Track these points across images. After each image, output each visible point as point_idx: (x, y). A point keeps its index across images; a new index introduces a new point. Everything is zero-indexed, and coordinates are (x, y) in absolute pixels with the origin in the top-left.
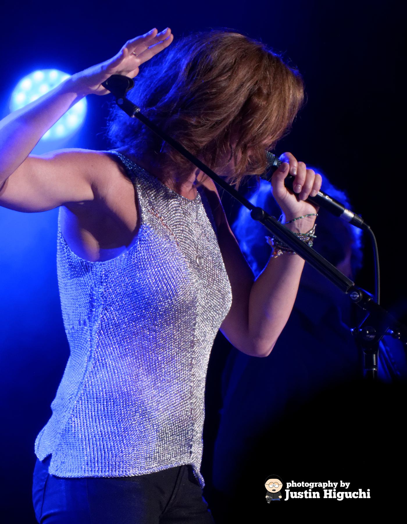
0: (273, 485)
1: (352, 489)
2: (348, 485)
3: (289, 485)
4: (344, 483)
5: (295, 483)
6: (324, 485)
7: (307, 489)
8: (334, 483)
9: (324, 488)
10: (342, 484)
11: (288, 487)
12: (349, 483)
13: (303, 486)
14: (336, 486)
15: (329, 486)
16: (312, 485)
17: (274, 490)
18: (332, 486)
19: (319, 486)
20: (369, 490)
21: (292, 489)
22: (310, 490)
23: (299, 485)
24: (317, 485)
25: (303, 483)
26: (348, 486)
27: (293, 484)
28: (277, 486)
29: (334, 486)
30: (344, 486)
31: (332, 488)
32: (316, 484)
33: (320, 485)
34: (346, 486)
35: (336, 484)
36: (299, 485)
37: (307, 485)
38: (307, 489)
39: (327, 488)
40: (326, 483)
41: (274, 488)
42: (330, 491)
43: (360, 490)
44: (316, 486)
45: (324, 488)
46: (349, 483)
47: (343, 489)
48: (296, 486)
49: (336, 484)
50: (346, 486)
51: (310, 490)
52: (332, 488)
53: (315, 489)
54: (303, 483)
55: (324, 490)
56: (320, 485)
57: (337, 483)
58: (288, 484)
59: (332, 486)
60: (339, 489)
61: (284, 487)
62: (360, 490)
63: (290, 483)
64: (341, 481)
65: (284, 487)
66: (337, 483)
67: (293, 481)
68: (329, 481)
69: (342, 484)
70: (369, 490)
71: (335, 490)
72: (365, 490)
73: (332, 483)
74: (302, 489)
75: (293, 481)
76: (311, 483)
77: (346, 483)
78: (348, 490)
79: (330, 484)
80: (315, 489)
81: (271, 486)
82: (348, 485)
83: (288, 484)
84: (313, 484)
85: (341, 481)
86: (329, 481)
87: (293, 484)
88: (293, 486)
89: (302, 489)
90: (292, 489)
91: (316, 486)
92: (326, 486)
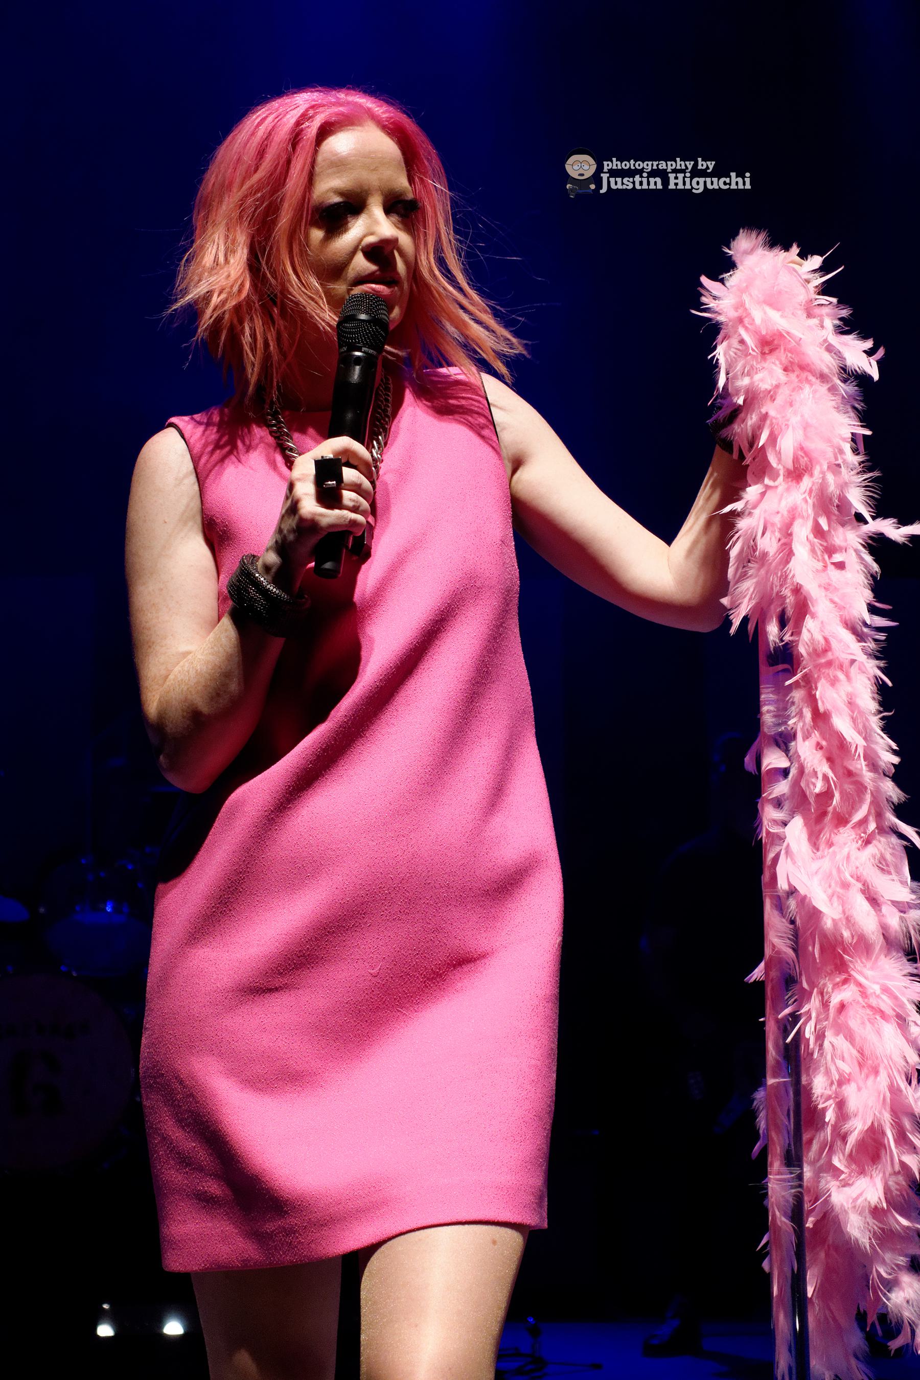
0: (580, 166)
1: (718, 173)
2: (711, 165)
4: (704, 163)
5: (619, 163)
6: (670, 166)
7: (640, 172)
8: (687, 163)
9: (669, 170)
10: (702, 164)
11: (606, 169)
12: (713, 163)
13: (633, 168)
14: (690, 167)
15: (678, 167)
16: (648, 166)
17: (582, 175)
18: (683, 167)
19: (660, 167)
20: (748, 174)
21: (613, 173)
22: (645, 175)
24: (657, 165)
25: (632, 162)
26: (711, 167)
27: (615, 164)
28: (586, 167)
29: (687, 168)
30: (704, 167)
31: (683, 171)
32: (655, 163)
33: (663, 165)
34: (708, 168)
35: (690, 165)
37: (640, 165)
38: (640, 172)
39: (675, 171)
40: (673, 163)
41: (581, 172)
42: (681, 176)
43: (733, 175)
44: (655, 167)
45: (669, 170)
46: (713, 163)
47: (703, 173)
48: (619, 167)
49: (690, 165)
50: (708, 168)
51: (645, 175)
52: (683, 171)
53: (653, 173)
54: (632, 162)
55: (670, 175)
56: (663, 165)
57: (692, 163)
58: (605, 163)
59: (683, 167)
61: (600, 169)
62: (733, 175)
63: (610, 163)
64: (700, 159)
65: (600, 169)
66: (692, 163)
67: (614, 159)
68: (678, 159)
69: (702, 164)
70: (748, 174)
71: (688, 175)
72: (741, 175)
73: (683, 163)
74: (631, 173)
75: (614, 159)
76: (646, 163)
77: (709, 163)
78: (711, 175)
79: (680, 164)
80: (653, 173)
81: (576, 167)
82: (711, 165)
83: (605, 163)
84: (650, 163)
85: (700, 159)
86: (678, 159)
87: (615, 164)
88: (615, 167)
89: (631, 173)
90: (613, 173)
91: (655, 167)
92: (673, 167)
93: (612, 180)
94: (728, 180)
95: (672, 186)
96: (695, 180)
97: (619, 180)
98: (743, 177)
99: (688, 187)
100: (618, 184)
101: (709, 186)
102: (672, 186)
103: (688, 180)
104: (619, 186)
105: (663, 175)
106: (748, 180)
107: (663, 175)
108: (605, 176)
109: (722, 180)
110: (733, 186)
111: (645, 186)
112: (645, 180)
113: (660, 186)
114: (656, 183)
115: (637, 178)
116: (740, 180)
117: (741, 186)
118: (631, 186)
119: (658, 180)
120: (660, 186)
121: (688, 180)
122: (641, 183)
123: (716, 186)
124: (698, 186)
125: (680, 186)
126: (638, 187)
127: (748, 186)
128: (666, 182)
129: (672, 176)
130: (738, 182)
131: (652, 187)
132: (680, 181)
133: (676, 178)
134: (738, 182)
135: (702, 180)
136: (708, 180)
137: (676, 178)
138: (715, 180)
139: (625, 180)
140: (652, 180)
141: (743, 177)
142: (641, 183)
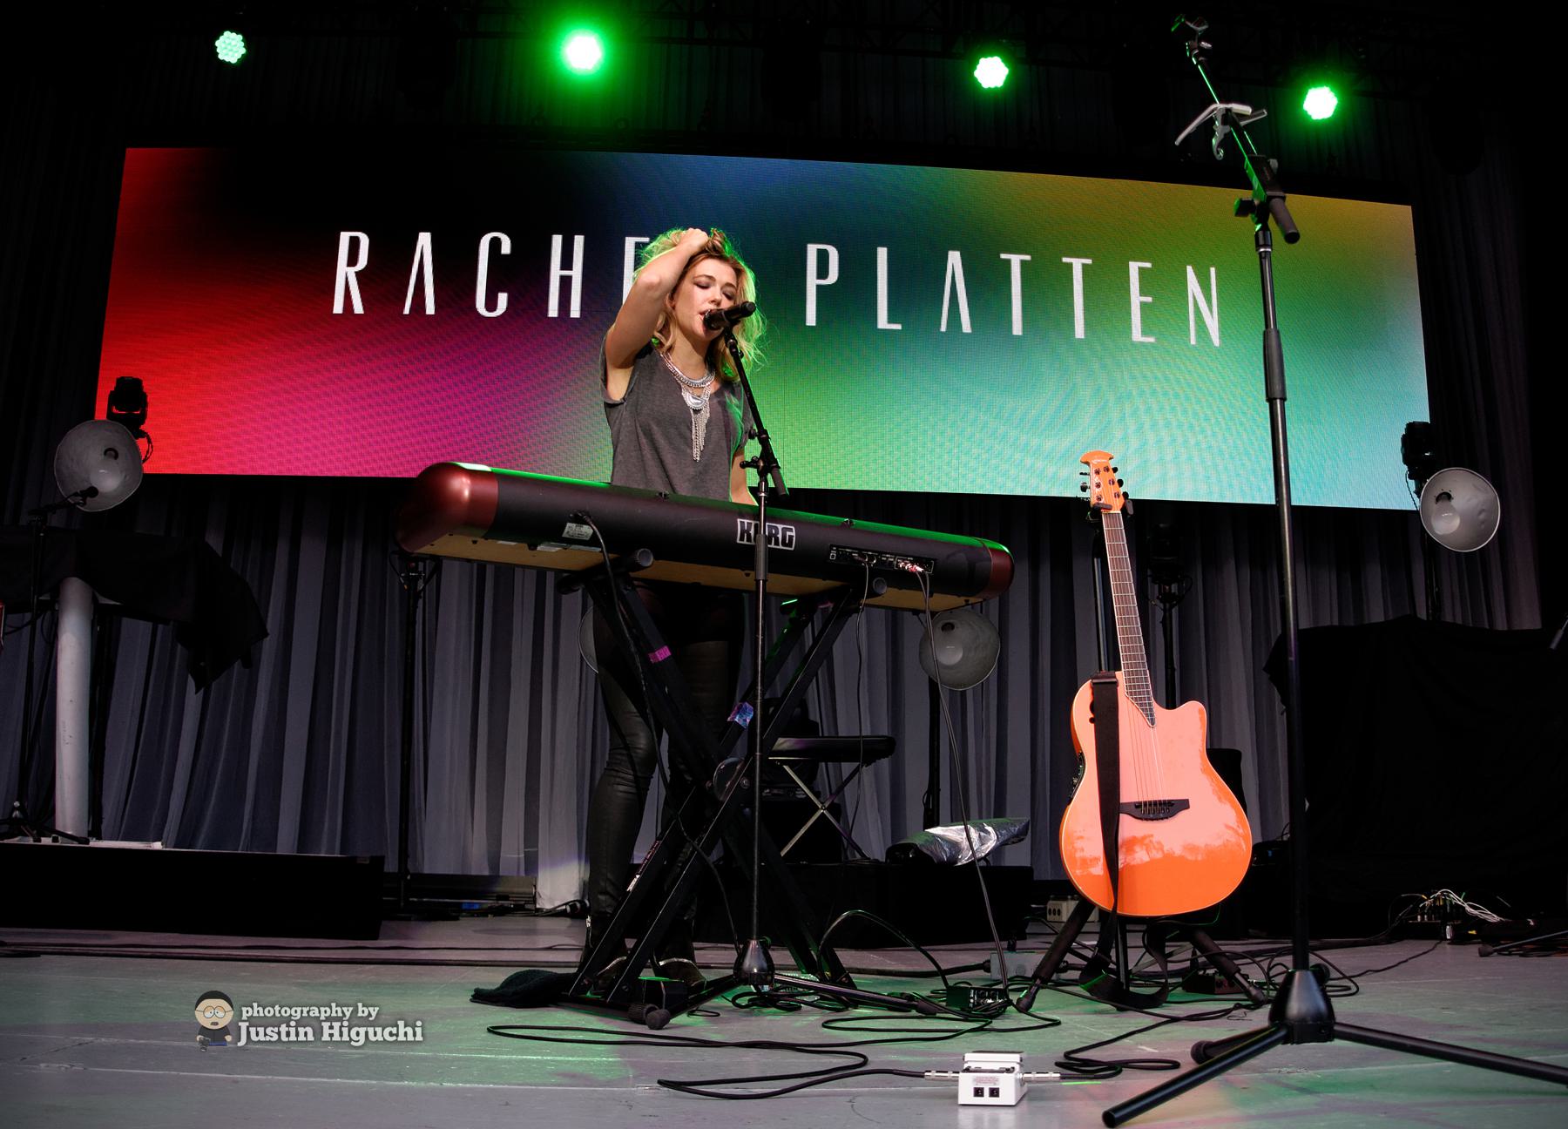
2: (374, 1011)
3: (246, 1012)
10: (362, 1011)
16: (296, 1013)
20: (419, 1023)
21: (253, 1022)
23: (269, 1012)
27: (257, 1011)
28: (221, 1014)
31: (340, 1019)
33: (315, 1012)
38: (287, 1021)
39: (328, 1019)
41: (214, 1020)
42: (337, 1025)
43: (401, 1023)
47: (366, 1022)
52: (340, 1019)
56: (315, 1012)
60: (355, 1021)
62: (401, 1023)
74: (276, 1022)
79: (336, 1010)
81: (208, 1014)
82: (374, 1011)
89: (276, 1022)
94: (394, 1030)
96: (354, 1031)
97: (261, 1030)
98: (413, 1027)
103: (345, 1030)
106: (419, 1031)
107: (316, 1025)
108: (244, 1025)
109: (387, 1030)
112: (293, 1031)
115: (283, 1028)
116: (409, 1030)
119: (309, 1030)
121: (345, 1030)
129: (326, 1025)
132: (336, 1032)
133: (331, 1027)
135: (362, 1030)
136: (371, 1030)
137: (331, 1027)
138: (379, 1030)
139: (269, 1030)
140: (302, 1031)
141: (413, 1027)
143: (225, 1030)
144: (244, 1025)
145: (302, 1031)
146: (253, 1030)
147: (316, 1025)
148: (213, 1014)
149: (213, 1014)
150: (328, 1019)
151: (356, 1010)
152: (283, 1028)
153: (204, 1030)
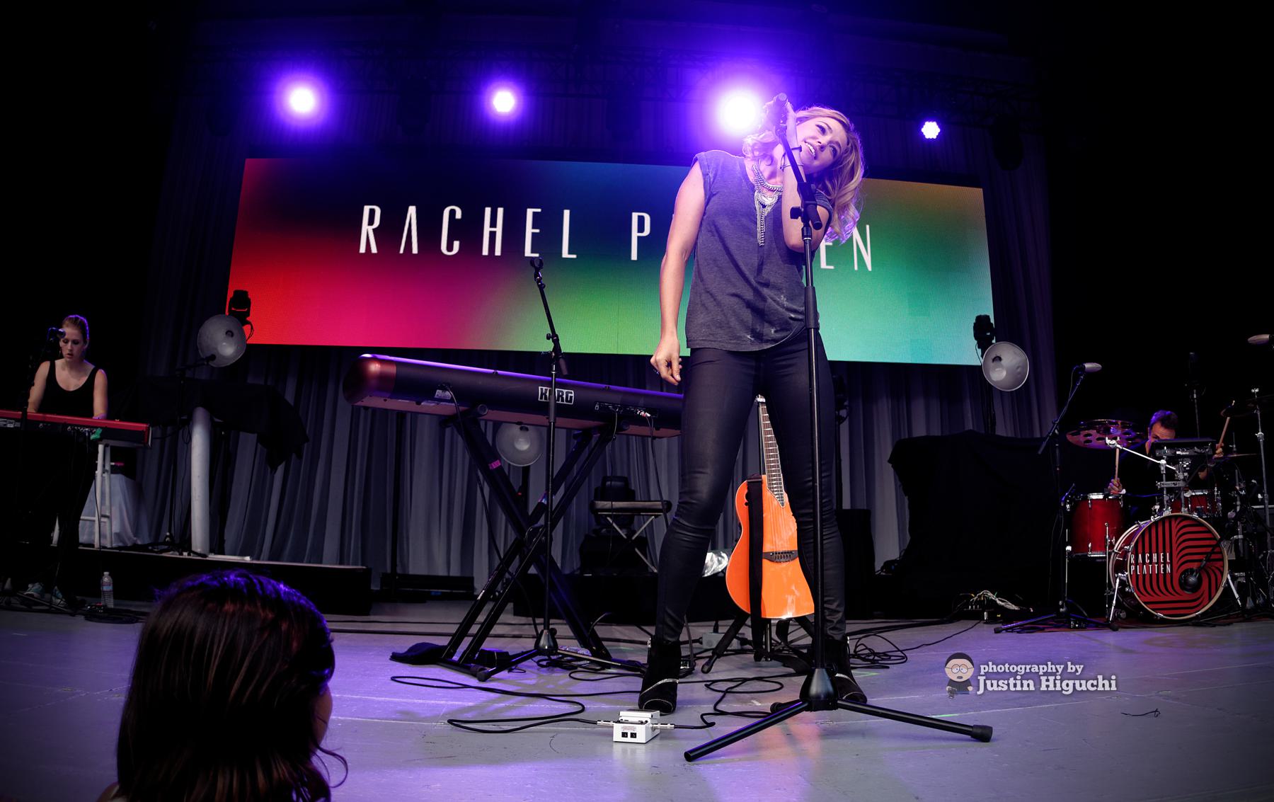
6: (1042, 669)
16: (1021, 669)
21: (989, 676)
23: (1001, 668)
27: (991, 668)
28: (964, 670)
31: (1052, 674)
33: (1035, 669)
36: (1001, 668)
37: (1014, 668)
38: (1015, 675)
39: (1045, 674)
42: (1052, 678)
43: (1100, 677)
47: (1073, 676)
52: (1052, 674)
56: (1035, 669)
60: (1065, 676)
61: (977, 672)
62: (1100, 677)
65: (977, 672)
78: (1079, 678)
79: (1051, 667)
87: (991, 668)
90: (989, 676)
93: (988, 682)
95: (1043, 688)
97: (995, 682)
98: (1110, 680)
99: (1058, 688)
100: (993, 686)
101: (1078, 688)
102: (1043, 688)
103: (1058, 683)
104: (995, 688)
105: (1036, 678)
106: (1113, 683)
108: (982, 679)
109: (1090, 682)
110: (1100, 688)
111: (1019, 688)
112: (1019, 683)
113: (1032, 688)
114: (1029, 685)
115: (1012, 681)
116: (1106, 682)
117: (1107, 688)
118: (1006, 688)
119: (1031, 682)
120: (1032, 688)
121: (1058, 683)
122: (1015, 685)
123: (1084, 688)
124: (1068, 687)
125: (1051, 688)
126: (1012, 688)
127: (1114, 688)
128: (1038, 683)
129: (1043, 679)
130: (1102, 684)
131: (1025, 688)
134: (1102, 684)
135: (1071, 683)
136: (1077, 682)
138: (1083, 682)
139: (1000, 683)
140: (1025, 682)
141: (1110, 680)
142: (1015, 685)
143: (967, 683)
144: (982, 679)
145: (1025, 682)
146: (988, 682)
147: (1036, 678)
148: (959, 670)
149: (959, 670)
150: (1045, 674)
151: (1066, 668)
152: (1012, 681)
153: (951, 682)
